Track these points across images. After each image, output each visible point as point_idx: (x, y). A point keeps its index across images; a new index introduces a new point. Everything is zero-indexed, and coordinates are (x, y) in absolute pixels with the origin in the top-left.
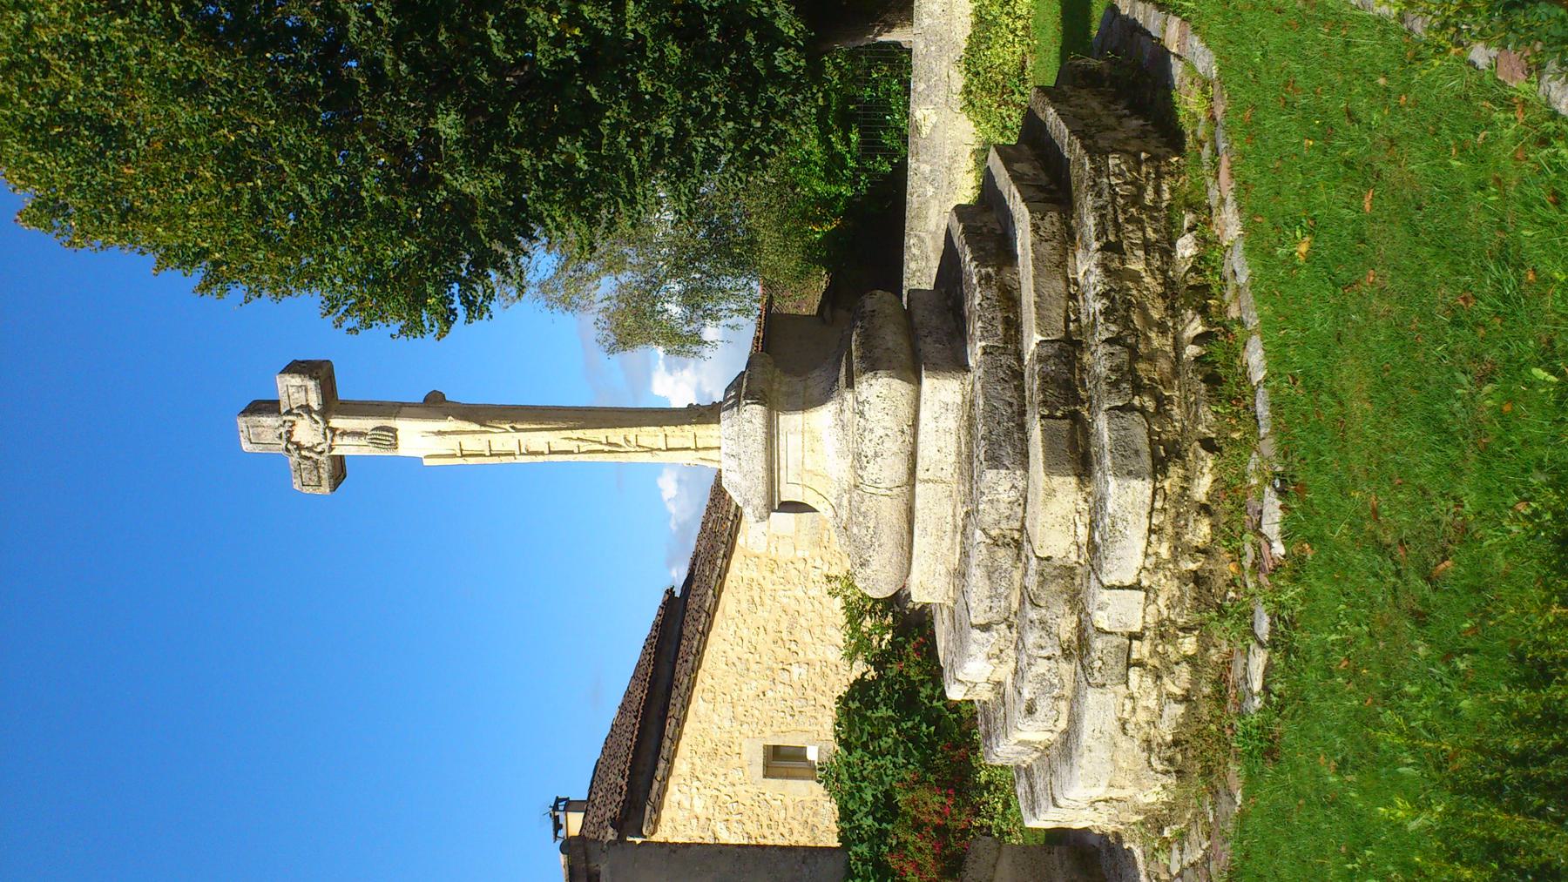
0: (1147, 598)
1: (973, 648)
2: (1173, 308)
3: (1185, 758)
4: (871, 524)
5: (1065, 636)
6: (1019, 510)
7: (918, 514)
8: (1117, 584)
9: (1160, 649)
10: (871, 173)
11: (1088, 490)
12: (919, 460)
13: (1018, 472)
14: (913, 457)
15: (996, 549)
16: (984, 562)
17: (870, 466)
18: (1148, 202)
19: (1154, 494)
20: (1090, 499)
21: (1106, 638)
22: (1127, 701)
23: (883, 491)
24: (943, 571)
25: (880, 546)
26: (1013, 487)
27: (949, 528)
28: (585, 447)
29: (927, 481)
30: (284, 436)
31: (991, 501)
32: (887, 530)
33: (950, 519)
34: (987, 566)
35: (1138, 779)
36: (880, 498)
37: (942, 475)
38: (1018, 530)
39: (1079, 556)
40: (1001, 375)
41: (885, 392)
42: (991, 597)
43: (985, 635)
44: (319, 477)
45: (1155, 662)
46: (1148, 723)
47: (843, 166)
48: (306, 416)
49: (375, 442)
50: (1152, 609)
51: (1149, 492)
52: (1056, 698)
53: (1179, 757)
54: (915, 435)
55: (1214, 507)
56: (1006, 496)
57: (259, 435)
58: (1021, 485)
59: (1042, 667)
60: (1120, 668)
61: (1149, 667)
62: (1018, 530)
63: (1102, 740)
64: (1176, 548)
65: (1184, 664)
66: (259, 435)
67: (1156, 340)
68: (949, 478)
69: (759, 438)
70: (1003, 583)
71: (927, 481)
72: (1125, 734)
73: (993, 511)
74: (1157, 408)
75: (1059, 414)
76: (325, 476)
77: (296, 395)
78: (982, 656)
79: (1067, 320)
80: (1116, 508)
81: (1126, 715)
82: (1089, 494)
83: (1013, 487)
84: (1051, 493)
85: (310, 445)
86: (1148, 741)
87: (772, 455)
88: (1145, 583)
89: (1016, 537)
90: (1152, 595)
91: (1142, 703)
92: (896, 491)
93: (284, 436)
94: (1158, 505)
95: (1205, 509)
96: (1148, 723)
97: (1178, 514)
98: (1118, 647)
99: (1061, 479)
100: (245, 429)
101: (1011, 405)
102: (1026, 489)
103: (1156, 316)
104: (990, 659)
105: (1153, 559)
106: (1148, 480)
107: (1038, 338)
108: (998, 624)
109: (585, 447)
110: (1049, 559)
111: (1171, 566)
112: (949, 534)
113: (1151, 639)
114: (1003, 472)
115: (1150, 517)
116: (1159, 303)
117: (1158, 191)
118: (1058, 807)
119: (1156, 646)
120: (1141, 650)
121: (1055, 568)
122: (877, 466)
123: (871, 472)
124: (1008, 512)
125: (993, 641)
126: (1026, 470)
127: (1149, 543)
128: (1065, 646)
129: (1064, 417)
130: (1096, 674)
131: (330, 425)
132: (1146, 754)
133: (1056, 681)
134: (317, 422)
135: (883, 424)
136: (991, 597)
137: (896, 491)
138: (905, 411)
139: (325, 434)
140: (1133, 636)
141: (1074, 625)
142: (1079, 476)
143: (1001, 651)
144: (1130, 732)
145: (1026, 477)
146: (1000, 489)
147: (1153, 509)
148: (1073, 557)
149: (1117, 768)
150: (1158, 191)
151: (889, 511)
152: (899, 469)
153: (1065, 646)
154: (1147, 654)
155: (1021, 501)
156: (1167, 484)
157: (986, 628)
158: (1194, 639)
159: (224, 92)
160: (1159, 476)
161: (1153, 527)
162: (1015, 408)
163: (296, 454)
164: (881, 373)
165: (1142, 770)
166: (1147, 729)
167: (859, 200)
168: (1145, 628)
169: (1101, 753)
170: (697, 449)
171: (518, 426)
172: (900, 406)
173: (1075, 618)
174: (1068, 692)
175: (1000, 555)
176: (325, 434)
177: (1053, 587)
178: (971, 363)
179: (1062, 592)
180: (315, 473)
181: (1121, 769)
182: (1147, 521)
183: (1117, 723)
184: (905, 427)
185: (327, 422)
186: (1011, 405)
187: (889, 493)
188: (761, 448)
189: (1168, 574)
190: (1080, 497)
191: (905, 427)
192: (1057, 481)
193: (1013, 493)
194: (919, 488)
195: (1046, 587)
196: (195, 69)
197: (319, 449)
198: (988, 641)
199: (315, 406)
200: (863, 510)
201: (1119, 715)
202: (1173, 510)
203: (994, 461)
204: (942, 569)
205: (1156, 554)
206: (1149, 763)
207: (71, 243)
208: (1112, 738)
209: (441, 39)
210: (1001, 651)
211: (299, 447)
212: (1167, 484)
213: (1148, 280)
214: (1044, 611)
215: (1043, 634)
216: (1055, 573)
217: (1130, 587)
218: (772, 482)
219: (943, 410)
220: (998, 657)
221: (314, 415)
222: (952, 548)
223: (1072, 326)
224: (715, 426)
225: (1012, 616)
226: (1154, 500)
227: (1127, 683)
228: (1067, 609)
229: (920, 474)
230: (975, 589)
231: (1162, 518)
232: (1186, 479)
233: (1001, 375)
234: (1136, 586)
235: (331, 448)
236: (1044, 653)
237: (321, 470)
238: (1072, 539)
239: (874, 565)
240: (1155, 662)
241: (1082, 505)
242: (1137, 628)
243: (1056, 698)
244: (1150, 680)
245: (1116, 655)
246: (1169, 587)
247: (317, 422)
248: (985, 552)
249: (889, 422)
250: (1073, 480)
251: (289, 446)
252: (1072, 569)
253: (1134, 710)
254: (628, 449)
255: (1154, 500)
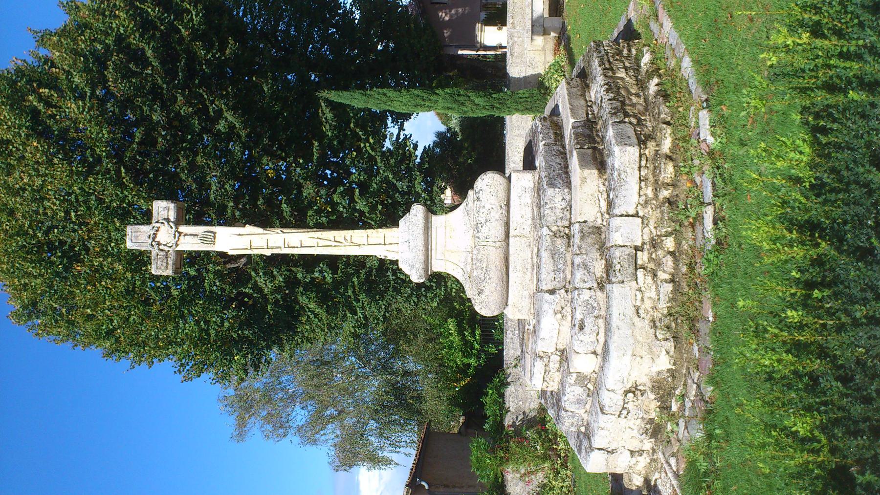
0: (643, 223)
1: (546, 306)
2: (642, 87)
3: (677, 324)
4: (484, 266)
5: (599, 274)
6: (568, 214)
7: (511, 259)
8: (625, 213)
9: (654, 256)
10: (486, 353)
11: (605, 177)
12: (511, 225)
13: (565, 190)
14: (507, 224)
15: (556, 239)
16: (549, 248)
17: (483, 230)
18: (625, 55)
19: (641, 156)
20: (607, 183)
21: (621, 249)
22: (638, 293)
23: (491, 244)
24: (527, 296)
25: (490, 279)
26: (563, 199)
27: (529, 266)
28: (321, 243)
29: (516, 236)
30: (151, 236)
31: (551, 208)
32: (493, 268)
33: (529, 260)
34: (551, 250)
35: (650, 348)
36: (490, 248)
37: (524, 232)
38: (567, 227)
39: (603, 220)
40: (554, 153)
41: (491, 182)
42: (554, 271)
43: (552, 297)
44: (167, 264)
45: (651, 265)
46: (652, 308)
47: (472, 348)
48: (166, 223)
49: (204, 240)
50: (646, 230)
51: (637, 154)
52: (597, 317)
53: (673, 325)
54: (508, 212)
55: (674, 157)
56: (559, 205)
57: (137, 236)
58: (568, 198)
59: (586, 295)
60: (631, 270)
61: (649, 269)
62: (567, 227)
63: (625, 321)
64: (656, 189)
65: (669, 256)
66: (137, 236)
67: (634, 99)
68: (528, 235)
69: (420, 225)
70: (561, 262)
71: (516, 236)
72: (639, 317)
73: (553, 214)
74: (638, 122)
75: (586, 147)
76: (170, 262)
77: (162, 212)
78: (551, 312)
79: (587, 114)
80: (620, 164)
81: (638, 303)
82: (605, 180)
83: (563, 199)
84: (584, 180)
85: (165, 243)
86: (653, 321)
87: (428, 240)
88: (641, 214)
89: (567, 232)
90: (646, 222)
91: (647, 295)
92: (498, 244)
93: (151, 236)
94: (643, 163)
95: (669, 158)
96: (652, 308)
97: (655, 168)
98: (629, 255)
99: (589, 171)
100: (130, 234)
101: (560, 164)
102: (570, 201)
103: (634, 92)
104: (556, 314)
105: (644, 198)
106: (636, 147)
107: (572, 120)
108: (559, 290)
109: (321, 243)
110: (585, 222)
111: (654, 202)
112: (530, 270)
113: (648, 250)
114: (557, 190)
115: (640, 171)
116: (635, 87)
117: (629, 50)
118: (604, 413)
119: (651, 254)
120: (643, 257)
121: (590, 228)
122: (487, 228)
123: (484, 231)
124: (561, 215)
125: (557, 301)
126: (570, 189)
127: (641, 188)
128: (599, 281)
129: (589, 148)
130: (618, 274)
131: (179, 230)
132: (653, 330)
133: (595, 305)
134: (171, 228)
135: (490, 201)
136: (554, 271)
137: (498, 244)
138: (502, 194)
139: (175, 235)
140: (637, 249)
141: (603, 266)
142: (599, 170)
143: (562, 308)
144: (642, 316)
145: (570, 193)
146: (556, 200)
147: (640, 167)
148: (599, 221)
149: (636, 341)
150: (629, 50)
151: (494, 256)
152: (500, 231)
153: (599, 281)
154: (646, 260)
155: (568, 208)
156: (647, 152)
157: (552, 292)
158: (672, 239)
159: (140, 218)
160: (642, 146)
161: (642, 178)
162: (562, 165)
163: (156, 247)
164: (487, 172)
165: (652, 342)
166: (652, 313)
167: (480, 368)
168: (644, 243)
169: (625, 330)
170: (385, 244)
171: (285, 230)
172: (500, 191)
173: (604, 262)
174: (603, 313)
175: (558, 243)
176: (175, 235)
177: (589, 240)
178: (537, 164)
179: (595, 244)
180: (165, 261)
181: (638, 342)
182: (638, 172)
183: (633, 309)
184: (503, 205)
185: (177, 228)
186: (560, 164)
187: (494, 244)
188: (422, 232)
189: (653, 206)
190: (601, 181)
191: (503, 205)
192: (587, 172)
193: (563, 203)
194: (511, 240)
195: (585, 240)
196: (127, 201)
197: (170, 245)
198: (554, 301)
199: (172, 218)
200: (479, 258)
201: (634, 303)
202: (652, 166)
203: (552, 185)
204: (526, 294)
205: (646, 195)
206: (656, 336)
207: (38, 334)
208: (631, 319)
209: (259, 203)
210: (562, 308)
211: (159, 244)
212: (647, 152)
213: (628, 79)
214: (585, 256)
215: (585, 272)
216: (590, 231)
217: (632, 216)
218: (428, 257)
219: (524, 192)
220: (561, 312)
221: (171, 223)
222: (531, 280)
223: (590, 116)
224: (395, 229)
225: (567, 284)
226: (640, 160)
227: (636, 280)
228: (598, 255)
229: (512, 233)
230: (545, 266)
231: (646, 171)
232: (657, 145)
233: (554, 153)
234: (636, 215)
235: (177, 245)
236: (587, 285)
237: (169, 259)
238: (597, 209)
239: (486, 292)
240: (651, 265)
241: (602, 188)
242: (639, 244)
243: (597, 317)
244: (650, 278)
245: (628, 260)
246: (653, 215)
247: (171, 228)
248: (549, 240)
249: (493, 200)
250: (595, 172)
251: (153, 243)
252: (599, 228)
253: (643, 300)
254: (346, 244)
255: (640, 160)
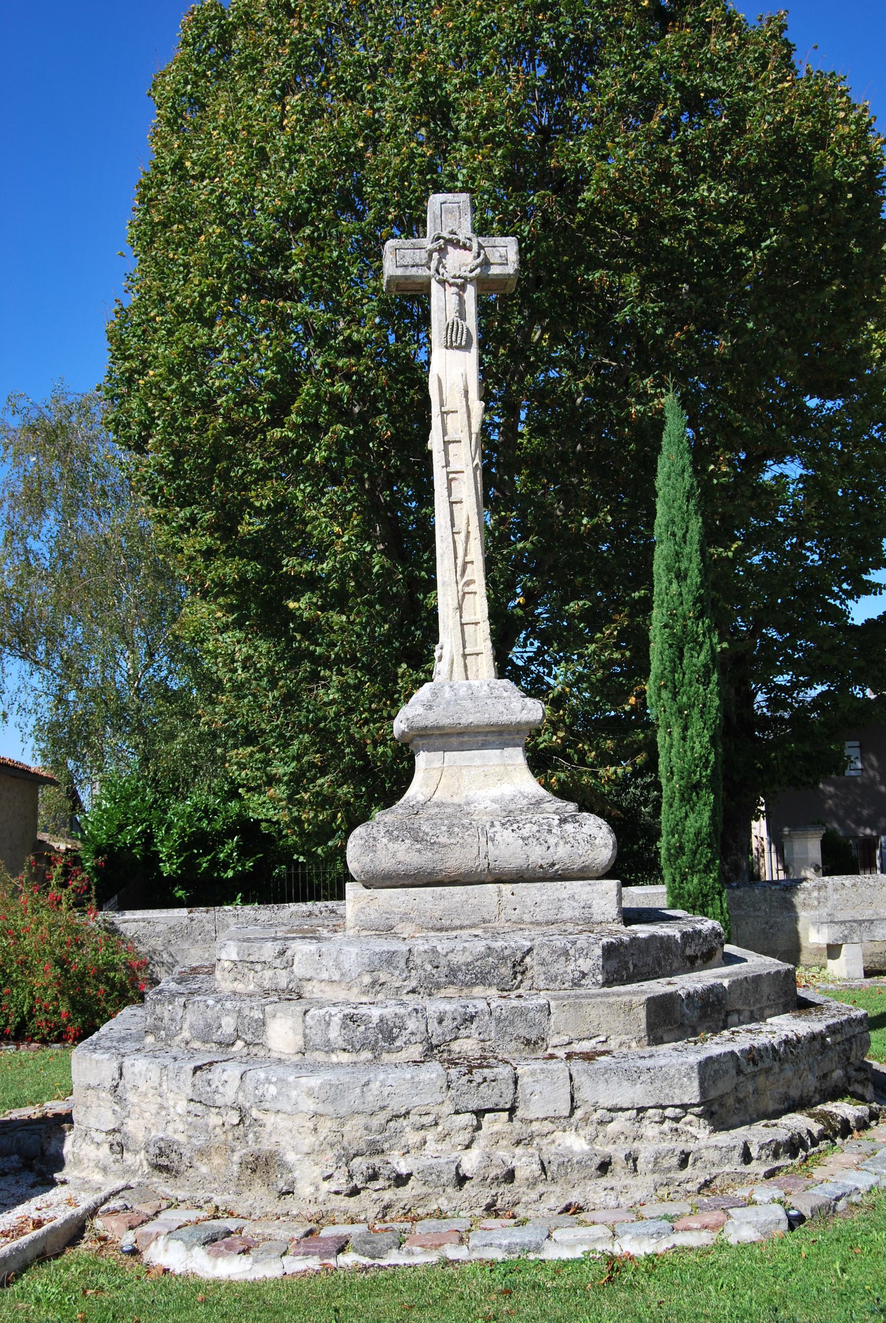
15: (510, 965)
28: (461, 538)
30: (454, 237)
48: (479, 261)
49: (451, 328)
77: (498, 254)
114: (600, 962)
118: (194, 1073)
134: (471, 271)
139: (460, 277)
147: (664, 1108)
170: (465, 656)
176: (460, 277)
184: (556, 867)
187: (482, 855)
191: (556, 867)
197: (441, 270)
211: (442, 251)
219: (582, 904)
224: (492, 672)
229: (506, 888)
247: (471, 271)
251: (442, 241)
